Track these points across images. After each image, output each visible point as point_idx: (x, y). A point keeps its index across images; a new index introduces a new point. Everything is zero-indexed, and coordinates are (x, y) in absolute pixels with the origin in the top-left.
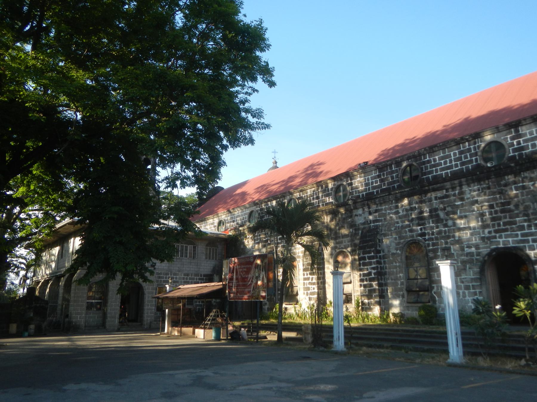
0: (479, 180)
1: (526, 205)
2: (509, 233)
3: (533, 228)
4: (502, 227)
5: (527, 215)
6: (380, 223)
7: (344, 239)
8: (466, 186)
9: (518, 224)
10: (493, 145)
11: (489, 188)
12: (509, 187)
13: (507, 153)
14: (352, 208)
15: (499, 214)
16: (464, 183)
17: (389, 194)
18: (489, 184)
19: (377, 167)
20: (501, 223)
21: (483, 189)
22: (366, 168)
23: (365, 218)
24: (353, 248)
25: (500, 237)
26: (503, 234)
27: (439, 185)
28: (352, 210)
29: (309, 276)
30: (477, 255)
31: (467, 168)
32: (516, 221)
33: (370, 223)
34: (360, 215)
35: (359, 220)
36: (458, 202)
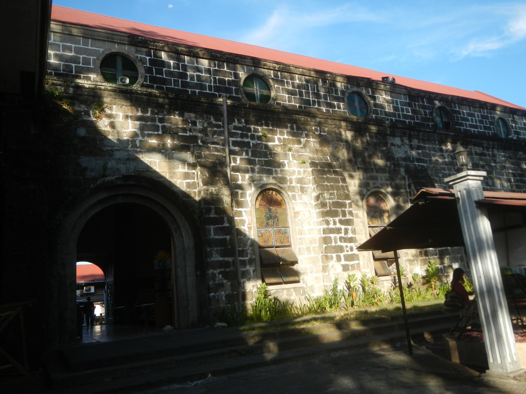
6: (425, 165)
7: (380, 175)
14: (389, 133)
16: (496, 146)
17: (433, 132)
19: (409, 92)
22: (396, 87)
23: (406, 152)
24: (395, 190)
27: (478, 140)
28: (386, 135)
29: (338, 225)
33: (413, 161)
34: (399, 147)
35: (399, 153)
36: (493, 163)
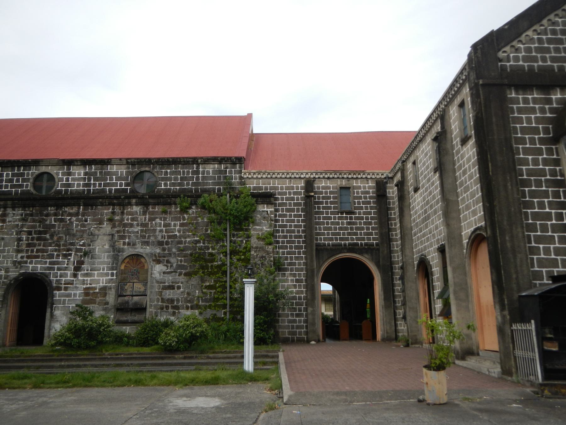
0: (24, 207)
1: (60, 236)
2: (40, 260)
3: (61, 257)
4: (35, 253)
5: (59, 246)
8: (11, 209)
9: (49, 253)
10: (45, 176)
11: (31, 215)
12: (49, 218)
13: (55, 187)
15: (35, 241)
18: (32, 211)
20: (35, 250)
21: (26, 215)
25: (31, 263)
26: (34, 260)
30: (5, 278)
31: (16, 192)
32: (48, 249)
